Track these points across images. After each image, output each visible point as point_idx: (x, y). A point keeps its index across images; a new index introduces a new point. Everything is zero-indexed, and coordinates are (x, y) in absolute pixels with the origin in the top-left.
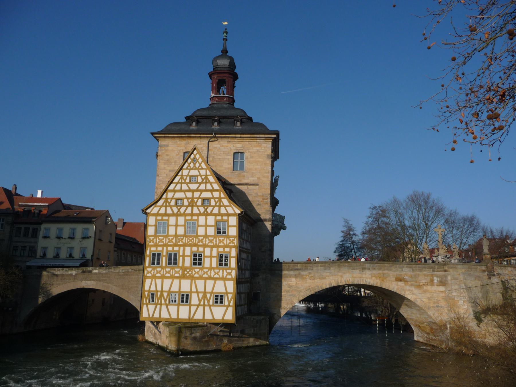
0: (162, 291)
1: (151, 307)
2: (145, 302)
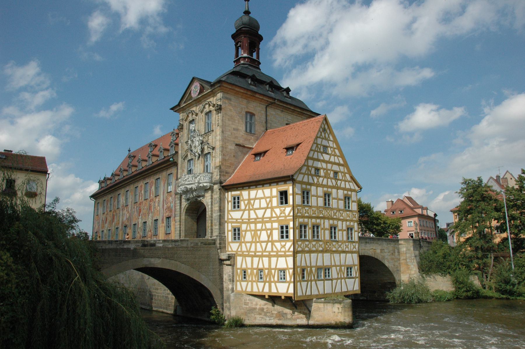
0: (311, 267)
1: (304, 284)
2: (298, 279)
